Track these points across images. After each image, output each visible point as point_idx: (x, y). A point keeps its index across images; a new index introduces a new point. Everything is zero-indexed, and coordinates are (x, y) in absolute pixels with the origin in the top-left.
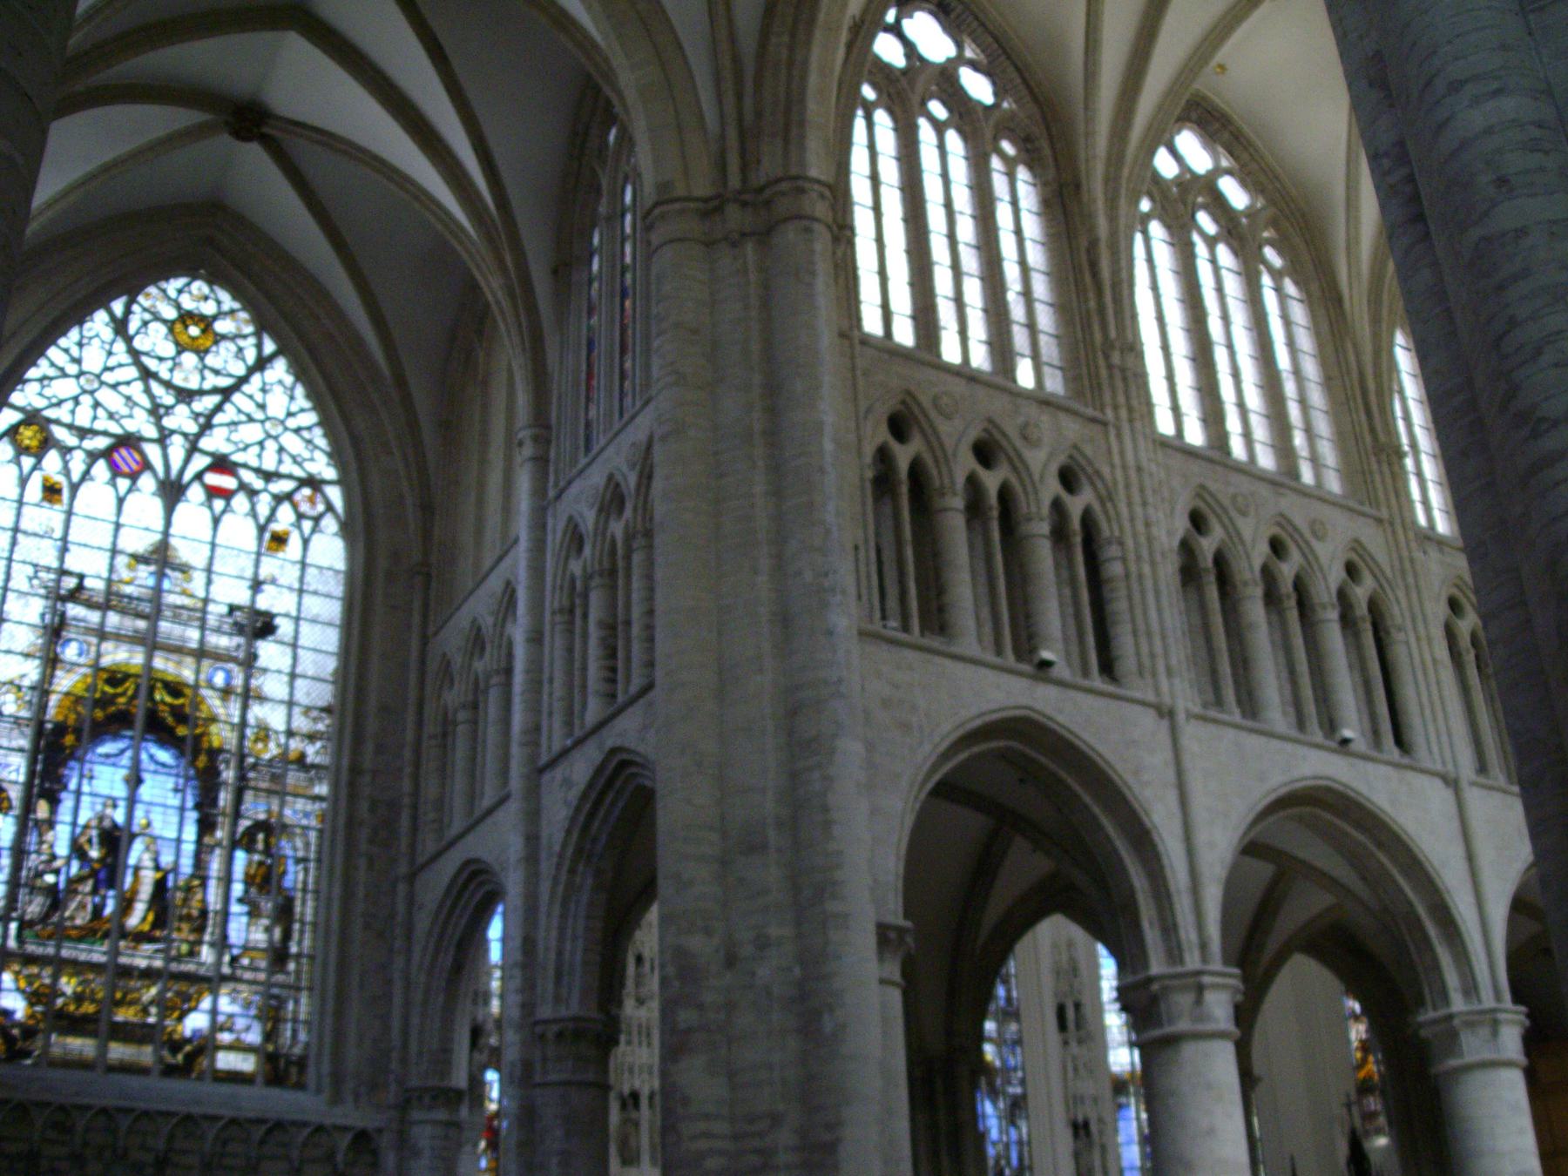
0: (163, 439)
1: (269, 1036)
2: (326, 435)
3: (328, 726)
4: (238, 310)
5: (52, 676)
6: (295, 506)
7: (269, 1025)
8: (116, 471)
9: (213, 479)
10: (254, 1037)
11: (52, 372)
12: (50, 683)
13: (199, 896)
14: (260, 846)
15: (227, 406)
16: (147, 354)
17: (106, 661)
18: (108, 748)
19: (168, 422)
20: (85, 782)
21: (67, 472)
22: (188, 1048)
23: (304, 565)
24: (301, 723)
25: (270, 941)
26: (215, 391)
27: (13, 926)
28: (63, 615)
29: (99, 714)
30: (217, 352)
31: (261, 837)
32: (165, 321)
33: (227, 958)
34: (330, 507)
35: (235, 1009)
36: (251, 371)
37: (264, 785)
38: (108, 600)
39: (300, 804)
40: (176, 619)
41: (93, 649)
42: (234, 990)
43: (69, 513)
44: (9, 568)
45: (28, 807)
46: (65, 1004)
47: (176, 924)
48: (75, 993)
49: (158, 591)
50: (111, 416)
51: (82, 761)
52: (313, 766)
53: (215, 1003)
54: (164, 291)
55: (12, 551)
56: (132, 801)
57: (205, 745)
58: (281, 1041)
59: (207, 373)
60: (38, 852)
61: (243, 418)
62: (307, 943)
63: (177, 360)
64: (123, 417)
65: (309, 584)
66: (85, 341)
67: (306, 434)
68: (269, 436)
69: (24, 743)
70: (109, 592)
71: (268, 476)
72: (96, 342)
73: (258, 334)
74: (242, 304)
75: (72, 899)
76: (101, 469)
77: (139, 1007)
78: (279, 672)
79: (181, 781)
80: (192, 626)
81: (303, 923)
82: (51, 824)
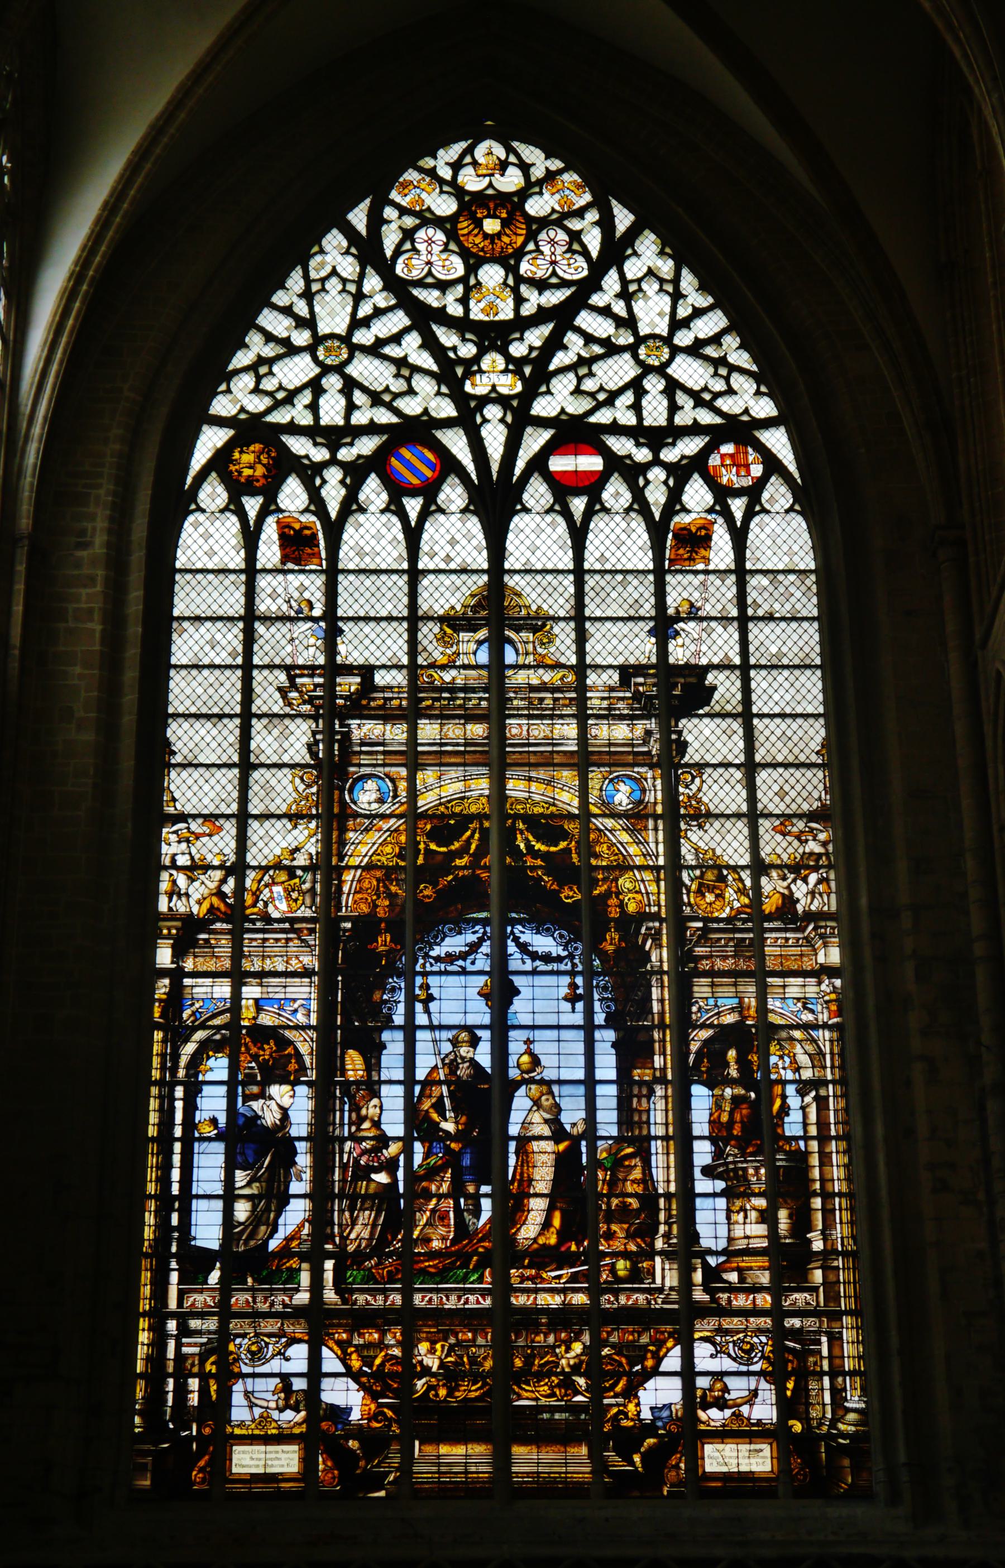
1: (787, 1407)
4: (560, 172)
5: (342, 843)
6: (711, 482)
7: (790, 1385)
9: (558, 464)
11: (269, 351)
12: (341, 858)
14: (734, 1073)
15: (574, 341)
16: (420, 283)
17: (426, 801)
18: (454, 944)
19: (477, 387)
20: (419, 1007)
21: (317, 503)
23: (741, 573)
25: (773, 1234)
26: (542, 315)
27: (329, 1265)
28: (347, 736)
29: (427, 891)
30: (538, 250)
31: (732, 1054)
32: (438, 222)
33: (698, 1277)
34: (772, 465)
35: (728, 1365)
37: (728, 964)
38: (414, 700)
39: (795, 987)
41: (402, 785)
42: (720, 1331)
43: (332, 573)
46: (430, 1388)
47: (603, 1227)
48: (442, 1365)
49: (497, 667)
50: (376, 399)
52: (810, 916)
53: (688, 1357)
54: (432, 173)
55: (248, 652)
57: (614, 913)
61: (597, 350)
62: (840, 1232)
63: (472, 281)
64: (396, 396)
65: (757, 605)
66: (315, 287)
67: (710, 351)
68: (647, 369)
69: (310, 961)
72: (334, 285)
73: (601, 204)
78: (726, 765)
79: (579, 981)
80: (561, 717)
81: (827, 1196)
82: (372, 1087)
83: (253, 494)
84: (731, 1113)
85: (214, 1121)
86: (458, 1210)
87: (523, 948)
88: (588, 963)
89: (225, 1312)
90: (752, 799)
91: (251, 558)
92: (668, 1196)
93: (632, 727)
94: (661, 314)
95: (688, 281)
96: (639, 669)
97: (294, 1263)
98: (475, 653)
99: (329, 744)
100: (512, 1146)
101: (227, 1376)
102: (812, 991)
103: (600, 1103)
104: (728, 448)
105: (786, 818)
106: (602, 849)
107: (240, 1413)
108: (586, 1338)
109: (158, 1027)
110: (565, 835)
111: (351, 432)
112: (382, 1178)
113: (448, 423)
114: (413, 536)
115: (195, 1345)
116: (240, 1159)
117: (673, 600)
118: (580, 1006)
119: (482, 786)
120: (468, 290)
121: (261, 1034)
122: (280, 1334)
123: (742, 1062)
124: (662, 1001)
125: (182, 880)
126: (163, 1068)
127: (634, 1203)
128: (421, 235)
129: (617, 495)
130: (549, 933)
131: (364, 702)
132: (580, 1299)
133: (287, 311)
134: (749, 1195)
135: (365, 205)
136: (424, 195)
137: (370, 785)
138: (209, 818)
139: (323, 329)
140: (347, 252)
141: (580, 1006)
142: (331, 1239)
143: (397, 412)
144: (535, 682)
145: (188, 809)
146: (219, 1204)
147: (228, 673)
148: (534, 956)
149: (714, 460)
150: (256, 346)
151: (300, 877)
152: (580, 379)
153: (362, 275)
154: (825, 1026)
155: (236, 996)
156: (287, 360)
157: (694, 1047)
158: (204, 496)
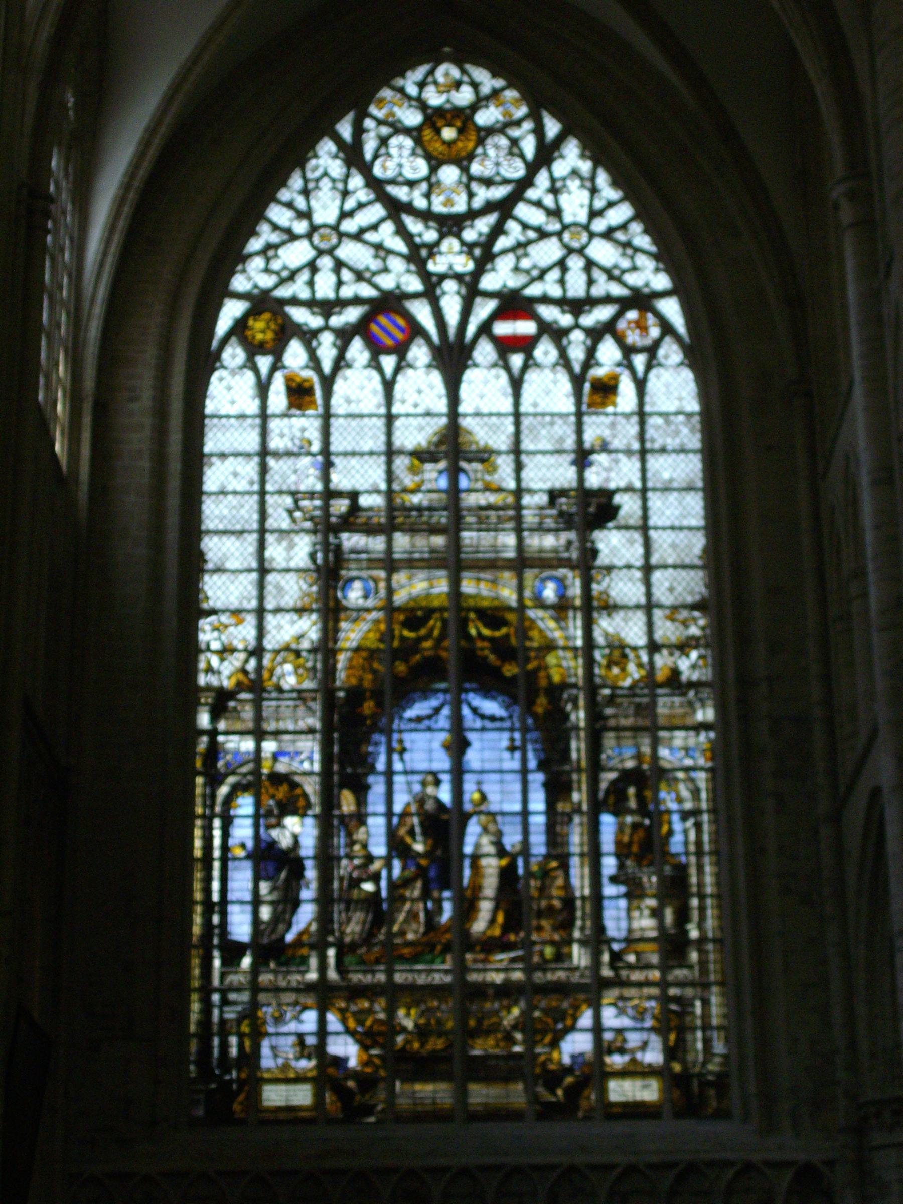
0: (431, 293)
1: (671, 1053)
2: (646, 231)
3: (703, 628)
5: (337, 630)
6: (620, 340)
7: (672, 1037)
8: (376, 349)
9: (502, 328)
10: (653, 1056)
11: (275, 238)
12: (336, 641)
13: (560, 882)
14: (633, 804)
15: (512, 226)
16: (393, 182)
17: (400, 598)
19: (436, 266)
20: (396, 757)
21: (315, 362)
22: (569, 1080)
23: (642, 415)
24: (666, 630)
25: (661, 926)
26: (489, 207)
27: (331, 952)
28: (338, 548)
29: (401, 668)
30: (485, 154)
31: (631, 791)
32: (407, 131)
33: (606, 957)
34: (667, 328)
35: (625, 1022)
36: (533, 169)
38: (391, 518)
40: (483, 525)
41: (382, 585)
42: (622, 998)
43: (327, 417)
44: (262, 504)
45: (329, 800)
46: (407, 1042)
47: (534, 922)
48: (417, 1025)
49: (454, 491)
50: (359, 276)
51: (389, 732)
52: (691, 685)
53: (597, 1018)
54: (402, 91)
55: (263, 482)
56: (458, 772)
57: (543, 683)
58: (690, 1057)
59: (475, 186)
60: (350, 857)
61: (532, 234)
62: (710, 923)
63: (434, 179)
64: (374, 274)
65: (653, 441)
66: (311, 185)
67: (620, 236)
69: (314, 722)
70: (391, 507)
71: (577, 306)
72: (325, 183)
73: (535, 116)
74: (505, 79)
75: (399, 910)
76: (357, 350)
77: (499, 1036)
78: (629, 567)
79: (517, 736)
80: (503, 530)
82: (360, 818)
83: (265, 353)
84: (631, 836)
85: (243, 846)
86: (427, 911)
87: (475, 711)
88: (523, 721)
89: (255, 988)
90: (649, 594)
91: (264, 406)
92: (583, 898)
93: (557, 538)
94: (582, 206)
95: (602, 178)
96: (563, 492)
97: (304, 951)
98: (436, 480)
99: (326, 553)
100: (467, 863)
101: (258, 1034)
102: (692, 742)
103: (532, 829)
104: (632, 315)
105: (675, 608)
106: (534, 634)
107: (267, 1061)
108: (523, 1004)
109: (200, 773)
110: (505, 623)
111: (341, 304)
112: (368, 887)
113: (416, 296)
114: (389, 386)
115: (233, 1012)
116: (263, 873)
117: (590, 437)
118: (518, 755)
119: (442, 586)
120: (431, 186)
121: (277, 778)
122: (296, 1004)
123: (640, 797)
124: (579, 750)
125: (215, 661)
126: (204, 806)
127: (557, 903)
128: (394, 142)
129: (546, 353)
130: (493, 698)
131: (352, 519)
132: (518, 976)
133: (290, 205)
134: (642, 896)
135: (350, 117)
136: (396, 109)
137: (357, 585)
138: (237, 612)
139: (318, 219)
140: (336, 156)
141: (518, 755)
142: (332, 932)
143: (376, 287)
144: (483, 502)
145: (219, 605)
146: (249, 908)
147: (247, 497)
148: (483, 717)
149: (621, 325)
150: (265, 235)
151: (304, 658)
152: (518, 259)
153: (347, 176)
154: (702, 769)
155: (258, 749)
156: (289, 245)
157: (603, 785)
158: (226, 355)
